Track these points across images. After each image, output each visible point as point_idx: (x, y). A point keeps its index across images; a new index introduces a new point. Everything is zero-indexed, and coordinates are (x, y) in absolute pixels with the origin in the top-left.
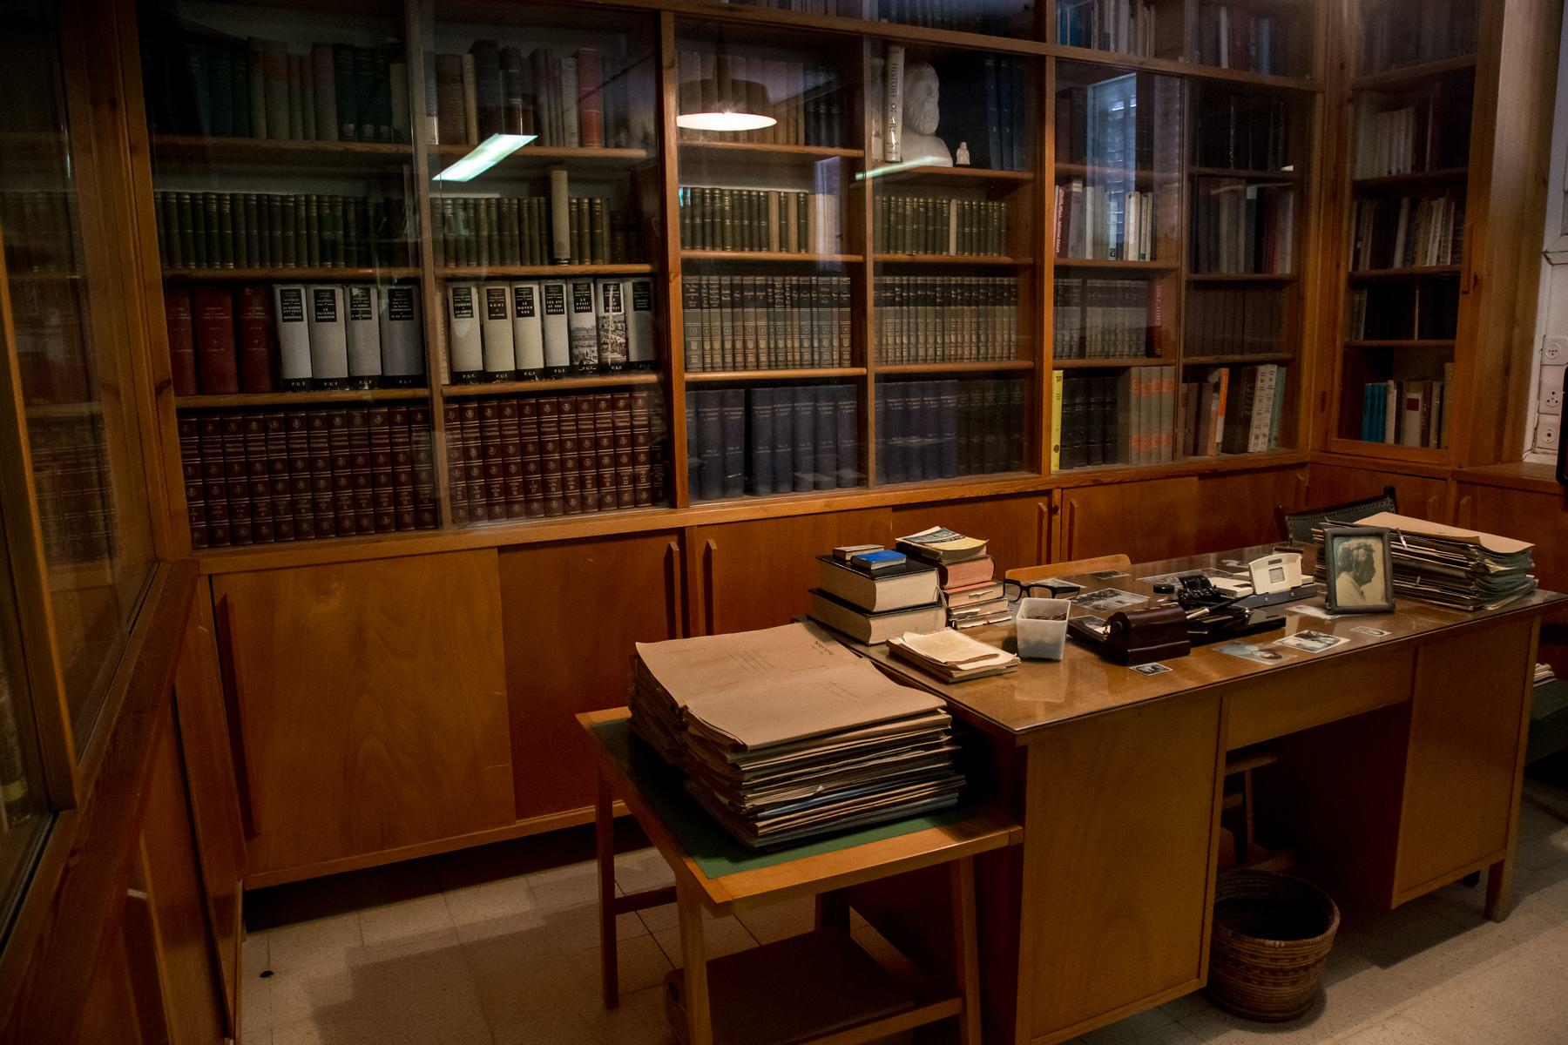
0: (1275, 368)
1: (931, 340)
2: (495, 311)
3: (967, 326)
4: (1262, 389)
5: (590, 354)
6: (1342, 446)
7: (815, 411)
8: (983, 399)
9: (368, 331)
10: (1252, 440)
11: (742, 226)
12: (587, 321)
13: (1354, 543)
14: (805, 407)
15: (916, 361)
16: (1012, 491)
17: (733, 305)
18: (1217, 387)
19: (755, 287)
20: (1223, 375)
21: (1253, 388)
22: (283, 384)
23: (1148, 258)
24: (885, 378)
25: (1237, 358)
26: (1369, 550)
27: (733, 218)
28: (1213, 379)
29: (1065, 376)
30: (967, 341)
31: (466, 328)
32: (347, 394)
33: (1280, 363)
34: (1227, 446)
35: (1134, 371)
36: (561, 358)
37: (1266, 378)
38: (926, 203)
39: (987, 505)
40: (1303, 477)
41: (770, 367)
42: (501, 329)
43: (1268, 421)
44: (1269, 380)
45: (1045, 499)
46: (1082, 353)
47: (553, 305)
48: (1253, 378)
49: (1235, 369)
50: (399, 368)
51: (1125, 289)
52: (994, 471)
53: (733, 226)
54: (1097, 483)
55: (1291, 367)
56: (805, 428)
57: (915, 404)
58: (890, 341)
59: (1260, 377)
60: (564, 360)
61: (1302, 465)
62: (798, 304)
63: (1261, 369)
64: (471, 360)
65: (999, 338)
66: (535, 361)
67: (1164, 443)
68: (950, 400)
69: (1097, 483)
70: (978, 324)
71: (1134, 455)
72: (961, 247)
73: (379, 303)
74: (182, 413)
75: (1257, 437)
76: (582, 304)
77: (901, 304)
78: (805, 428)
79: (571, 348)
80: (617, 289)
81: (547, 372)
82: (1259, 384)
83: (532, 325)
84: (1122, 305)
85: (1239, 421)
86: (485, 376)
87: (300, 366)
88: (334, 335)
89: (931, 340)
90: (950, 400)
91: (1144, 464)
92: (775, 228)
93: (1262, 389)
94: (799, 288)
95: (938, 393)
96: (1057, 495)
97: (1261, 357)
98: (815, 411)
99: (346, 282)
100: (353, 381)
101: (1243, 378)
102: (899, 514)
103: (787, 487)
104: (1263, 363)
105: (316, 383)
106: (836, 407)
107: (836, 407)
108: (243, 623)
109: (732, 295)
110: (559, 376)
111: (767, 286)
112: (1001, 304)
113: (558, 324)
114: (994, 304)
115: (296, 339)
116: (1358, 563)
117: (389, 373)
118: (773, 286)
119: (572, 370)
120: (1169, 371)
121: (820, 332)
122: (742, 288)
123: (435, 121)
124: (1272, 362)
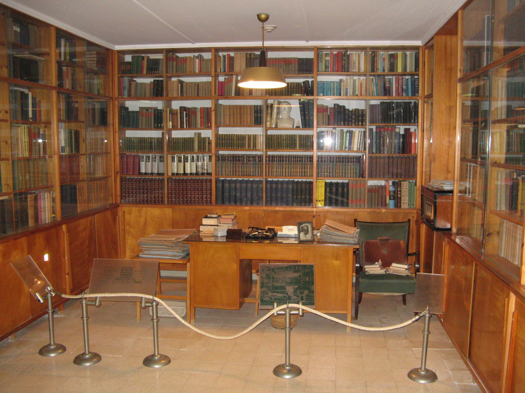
1: (287, 170)
5: (200, 171)
9: (156, 164)
13: (304, 225)
22: (140, 174)
26: (307, 227)
36: (194, 171)
37: (405, 185)
87: (143, 171)
100: (152, 174)
103: (233, 203)
105: (146, 174)
117: (159, 172)
119: (197, 174)
123: (171, 123)
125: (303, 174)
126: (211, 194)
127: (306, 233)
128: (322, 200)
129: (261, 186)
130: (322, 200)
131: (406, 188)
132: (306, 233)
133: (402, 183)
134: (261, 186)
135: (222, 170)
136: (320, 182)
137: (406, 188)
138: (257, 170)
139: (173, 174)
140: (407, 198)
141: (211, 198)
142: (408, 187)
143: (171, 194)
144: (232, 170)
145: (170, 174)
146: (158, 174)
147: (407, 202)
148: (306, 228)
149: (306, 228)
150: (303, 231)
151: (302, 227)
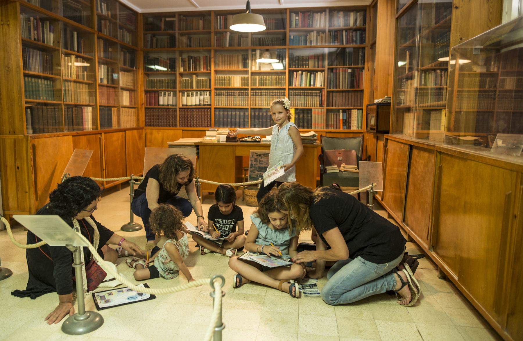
2: (188, 96)
5: (202, 103)
7: (240, 114)
9: (171, 98)
12: (202, 98)
14: (238, 113)
22: (159, 105)
23: (323, 86)
24: (251, 109)
25: (344, 108)
31: (185, 98)
32: (167, 107)
33: (358, 109)
35: (313, 110)
42: (189, 98)
44: (355, 113)
47: (197, 95)
50: (174, 104)
56: (238, 117)
57: (257, 113)
60: (198, 104)
63: (352, 110)
64: (185, 103)
73: (172, 93)
74: (145, 108)
76: (201, 95)
78: (238, 117)
81: (195, 105)
83: (193, 98)
86: (187, 105)
87: (161, 103)
88: (166, 98)
97: (352, 108)
98: (240, 114)
99: (168, 91)
101: (348, 112)
105: (163, 105)
108: (149, 136)
113: (197, 98)
115: (161, 98)
119: (199, 105)
126: (211, 119)
129: (246, 114)
133: (352, 110)
139: (183, 105)
140: (356, 122)
141: (211, 122)
143: (182, 120)
145: (181, 106)
146: (172, 105)
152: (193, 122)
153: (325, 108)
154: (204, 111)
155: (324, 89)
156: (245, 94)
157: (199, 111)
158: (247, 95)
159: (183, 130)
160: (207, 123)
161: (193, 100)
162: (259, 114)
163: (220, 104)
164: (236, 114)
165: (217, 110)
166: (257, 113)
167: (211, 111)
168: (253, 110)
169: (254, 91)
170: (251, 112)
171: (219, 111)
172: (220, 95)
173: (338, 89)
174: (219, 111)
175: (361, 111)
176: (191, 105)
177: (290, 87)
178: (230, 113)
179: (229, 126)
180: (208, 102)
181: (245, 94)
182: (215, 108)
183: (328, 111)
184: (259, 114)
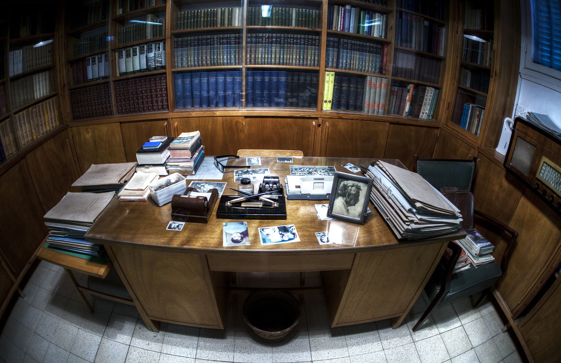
0: (433, 89)
1: (278, 56)
3: (295, 52)
4: (427, 96)
6: (450, 124)
8: (299, 80)
10: (421, 114)
11: (207, 20)
12: (152, 55)
15: (271, 64)
16: (298, 116)
17: (198, 45)
18: (409, 91)
19: (207, 39)
20: (411, 87)
21: (424, 94)
23: (383, 37)
24: (248, 69)
26: (359, 189)
27: (204, 18)
28: (409, 88)
29: (336, 75)
30: (292, 59)
33: (436, 88)
34: (411, 113)
35: (368, 78)
36: (145, 67)
37: (429, 92)
38: (282, 9)
39: (289, 120)
40: (437, 132)
41: (211, 65)
43: (428, 108)
45: (316, 121)
46: (337, 67)
47: (142, 52)
48: (424, 91)
49: (417, 86)
51: (370, 47)
52: (303, 106)
53: (204, 20)
54: (340, 118)
55: (438, 89)
58: (260, 56)
59: (427, 91)
61: (438, 128)
62: (223, 44)
63: (428, 88)
65: (309, 58)
66: (138, 68)
67: (380, 107)
68: (283, 79)
69: (340, 118)
70: (300, 51)
71: (366, 109)
72: (298, 24)
75: (423, 113)
76: (150, 50)
77: (265, 43)
78: (221, 86)
79: (147, 63)
80: (159, 44)
81: (140, 71)
82: (426, 94)
84: (369, 52)
85: (417, 103)
89: (278, 56)
90: (283, 79)
91: (370, 114)
92: (219, 20)
93: (427, 96)
94: (223, 38)
95: (278, 75)
96: (320, 120)
97: (429, 84)
101: (420, 89)
102: (248, 119)
104: (429, 86)
106: (234, 79)
107: (234, 79)
109: (198, 42)
110: (143, 72)
111: (211, 38)
112: (311, 45)
113: (144, 57)
114: (308, 45)
116: (349, 194)
118: (213, 38)
119: (148, 69)
120: (384, 81)
121: (230, 53)
122: (202, 39)
124: (433, 87)
125: (301, 62)
127: (351, 200)
128: (330, 102)
129: (238, 79)
130: (330, 102)
131: (430, 96)
132: (351, 200)
134: (238, 79)
135: (182, 60)
136: (328, 75)
137: (430, 96)
138: (233, 57)
140: (428, 107)
142: (432, 95)
144: (196, 59)
147: (427, 112)
148: (353, 190)
149: (353, 190)
150: (343, 195)
151: (345, 187)
152: (138, 103)
153: (390, 77)
154: (155, 80)
155: (388, 43)
156: (233, 41)
157: (145, 81)
158: (240, 43)
159: (121, 123)
160: (162, 102)
161: (137, 62)
162: (263, 81)
163: (185, 64)
164: (216, 83)
165: (179, 76)
166: (259, 79)
167: (166, 78)
168: (250, 72)
169: (254, 35)
170: (247, 76)
171: (183, 78)
172: (183, 45)
173: (408, 49)
174: (183, 78)
175: (437, 91)
176: (134, 72)
177: (329, 31)
178: (205, 80)
179: (204, 106)
180: (161, 63)
181: (233, 41)
182: (174, 73)
183: (394, 83)
184: (263, 81)
